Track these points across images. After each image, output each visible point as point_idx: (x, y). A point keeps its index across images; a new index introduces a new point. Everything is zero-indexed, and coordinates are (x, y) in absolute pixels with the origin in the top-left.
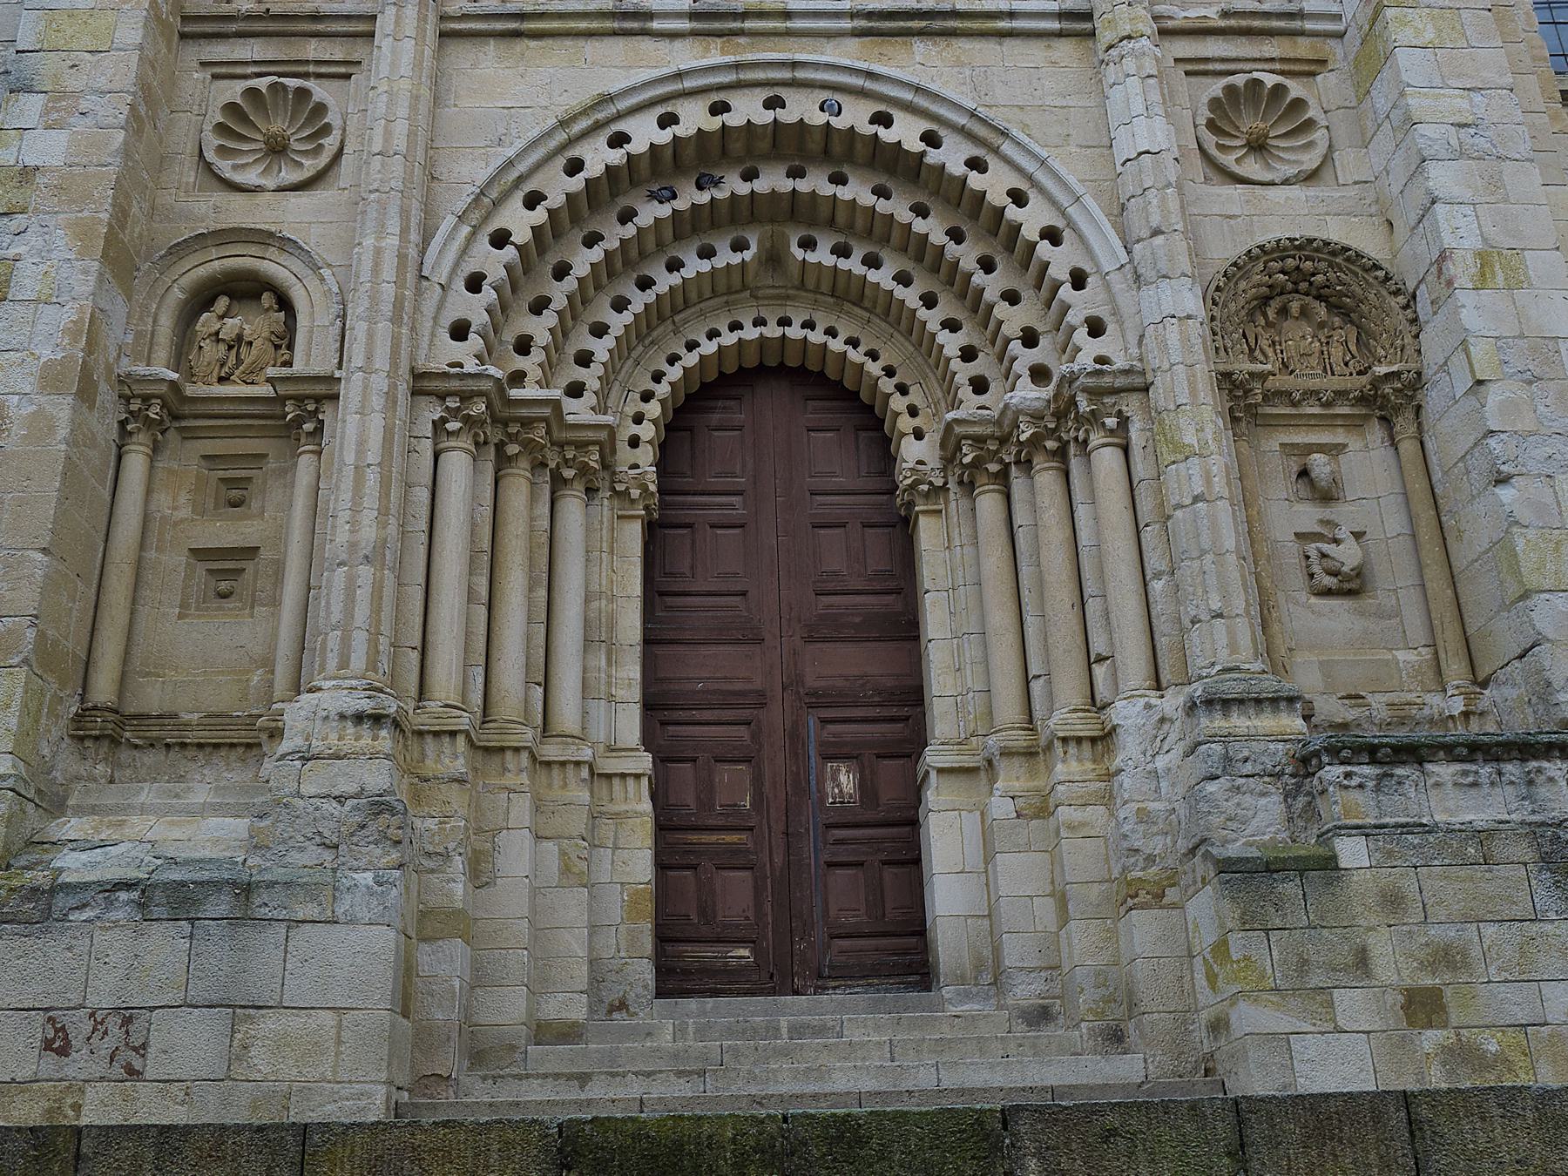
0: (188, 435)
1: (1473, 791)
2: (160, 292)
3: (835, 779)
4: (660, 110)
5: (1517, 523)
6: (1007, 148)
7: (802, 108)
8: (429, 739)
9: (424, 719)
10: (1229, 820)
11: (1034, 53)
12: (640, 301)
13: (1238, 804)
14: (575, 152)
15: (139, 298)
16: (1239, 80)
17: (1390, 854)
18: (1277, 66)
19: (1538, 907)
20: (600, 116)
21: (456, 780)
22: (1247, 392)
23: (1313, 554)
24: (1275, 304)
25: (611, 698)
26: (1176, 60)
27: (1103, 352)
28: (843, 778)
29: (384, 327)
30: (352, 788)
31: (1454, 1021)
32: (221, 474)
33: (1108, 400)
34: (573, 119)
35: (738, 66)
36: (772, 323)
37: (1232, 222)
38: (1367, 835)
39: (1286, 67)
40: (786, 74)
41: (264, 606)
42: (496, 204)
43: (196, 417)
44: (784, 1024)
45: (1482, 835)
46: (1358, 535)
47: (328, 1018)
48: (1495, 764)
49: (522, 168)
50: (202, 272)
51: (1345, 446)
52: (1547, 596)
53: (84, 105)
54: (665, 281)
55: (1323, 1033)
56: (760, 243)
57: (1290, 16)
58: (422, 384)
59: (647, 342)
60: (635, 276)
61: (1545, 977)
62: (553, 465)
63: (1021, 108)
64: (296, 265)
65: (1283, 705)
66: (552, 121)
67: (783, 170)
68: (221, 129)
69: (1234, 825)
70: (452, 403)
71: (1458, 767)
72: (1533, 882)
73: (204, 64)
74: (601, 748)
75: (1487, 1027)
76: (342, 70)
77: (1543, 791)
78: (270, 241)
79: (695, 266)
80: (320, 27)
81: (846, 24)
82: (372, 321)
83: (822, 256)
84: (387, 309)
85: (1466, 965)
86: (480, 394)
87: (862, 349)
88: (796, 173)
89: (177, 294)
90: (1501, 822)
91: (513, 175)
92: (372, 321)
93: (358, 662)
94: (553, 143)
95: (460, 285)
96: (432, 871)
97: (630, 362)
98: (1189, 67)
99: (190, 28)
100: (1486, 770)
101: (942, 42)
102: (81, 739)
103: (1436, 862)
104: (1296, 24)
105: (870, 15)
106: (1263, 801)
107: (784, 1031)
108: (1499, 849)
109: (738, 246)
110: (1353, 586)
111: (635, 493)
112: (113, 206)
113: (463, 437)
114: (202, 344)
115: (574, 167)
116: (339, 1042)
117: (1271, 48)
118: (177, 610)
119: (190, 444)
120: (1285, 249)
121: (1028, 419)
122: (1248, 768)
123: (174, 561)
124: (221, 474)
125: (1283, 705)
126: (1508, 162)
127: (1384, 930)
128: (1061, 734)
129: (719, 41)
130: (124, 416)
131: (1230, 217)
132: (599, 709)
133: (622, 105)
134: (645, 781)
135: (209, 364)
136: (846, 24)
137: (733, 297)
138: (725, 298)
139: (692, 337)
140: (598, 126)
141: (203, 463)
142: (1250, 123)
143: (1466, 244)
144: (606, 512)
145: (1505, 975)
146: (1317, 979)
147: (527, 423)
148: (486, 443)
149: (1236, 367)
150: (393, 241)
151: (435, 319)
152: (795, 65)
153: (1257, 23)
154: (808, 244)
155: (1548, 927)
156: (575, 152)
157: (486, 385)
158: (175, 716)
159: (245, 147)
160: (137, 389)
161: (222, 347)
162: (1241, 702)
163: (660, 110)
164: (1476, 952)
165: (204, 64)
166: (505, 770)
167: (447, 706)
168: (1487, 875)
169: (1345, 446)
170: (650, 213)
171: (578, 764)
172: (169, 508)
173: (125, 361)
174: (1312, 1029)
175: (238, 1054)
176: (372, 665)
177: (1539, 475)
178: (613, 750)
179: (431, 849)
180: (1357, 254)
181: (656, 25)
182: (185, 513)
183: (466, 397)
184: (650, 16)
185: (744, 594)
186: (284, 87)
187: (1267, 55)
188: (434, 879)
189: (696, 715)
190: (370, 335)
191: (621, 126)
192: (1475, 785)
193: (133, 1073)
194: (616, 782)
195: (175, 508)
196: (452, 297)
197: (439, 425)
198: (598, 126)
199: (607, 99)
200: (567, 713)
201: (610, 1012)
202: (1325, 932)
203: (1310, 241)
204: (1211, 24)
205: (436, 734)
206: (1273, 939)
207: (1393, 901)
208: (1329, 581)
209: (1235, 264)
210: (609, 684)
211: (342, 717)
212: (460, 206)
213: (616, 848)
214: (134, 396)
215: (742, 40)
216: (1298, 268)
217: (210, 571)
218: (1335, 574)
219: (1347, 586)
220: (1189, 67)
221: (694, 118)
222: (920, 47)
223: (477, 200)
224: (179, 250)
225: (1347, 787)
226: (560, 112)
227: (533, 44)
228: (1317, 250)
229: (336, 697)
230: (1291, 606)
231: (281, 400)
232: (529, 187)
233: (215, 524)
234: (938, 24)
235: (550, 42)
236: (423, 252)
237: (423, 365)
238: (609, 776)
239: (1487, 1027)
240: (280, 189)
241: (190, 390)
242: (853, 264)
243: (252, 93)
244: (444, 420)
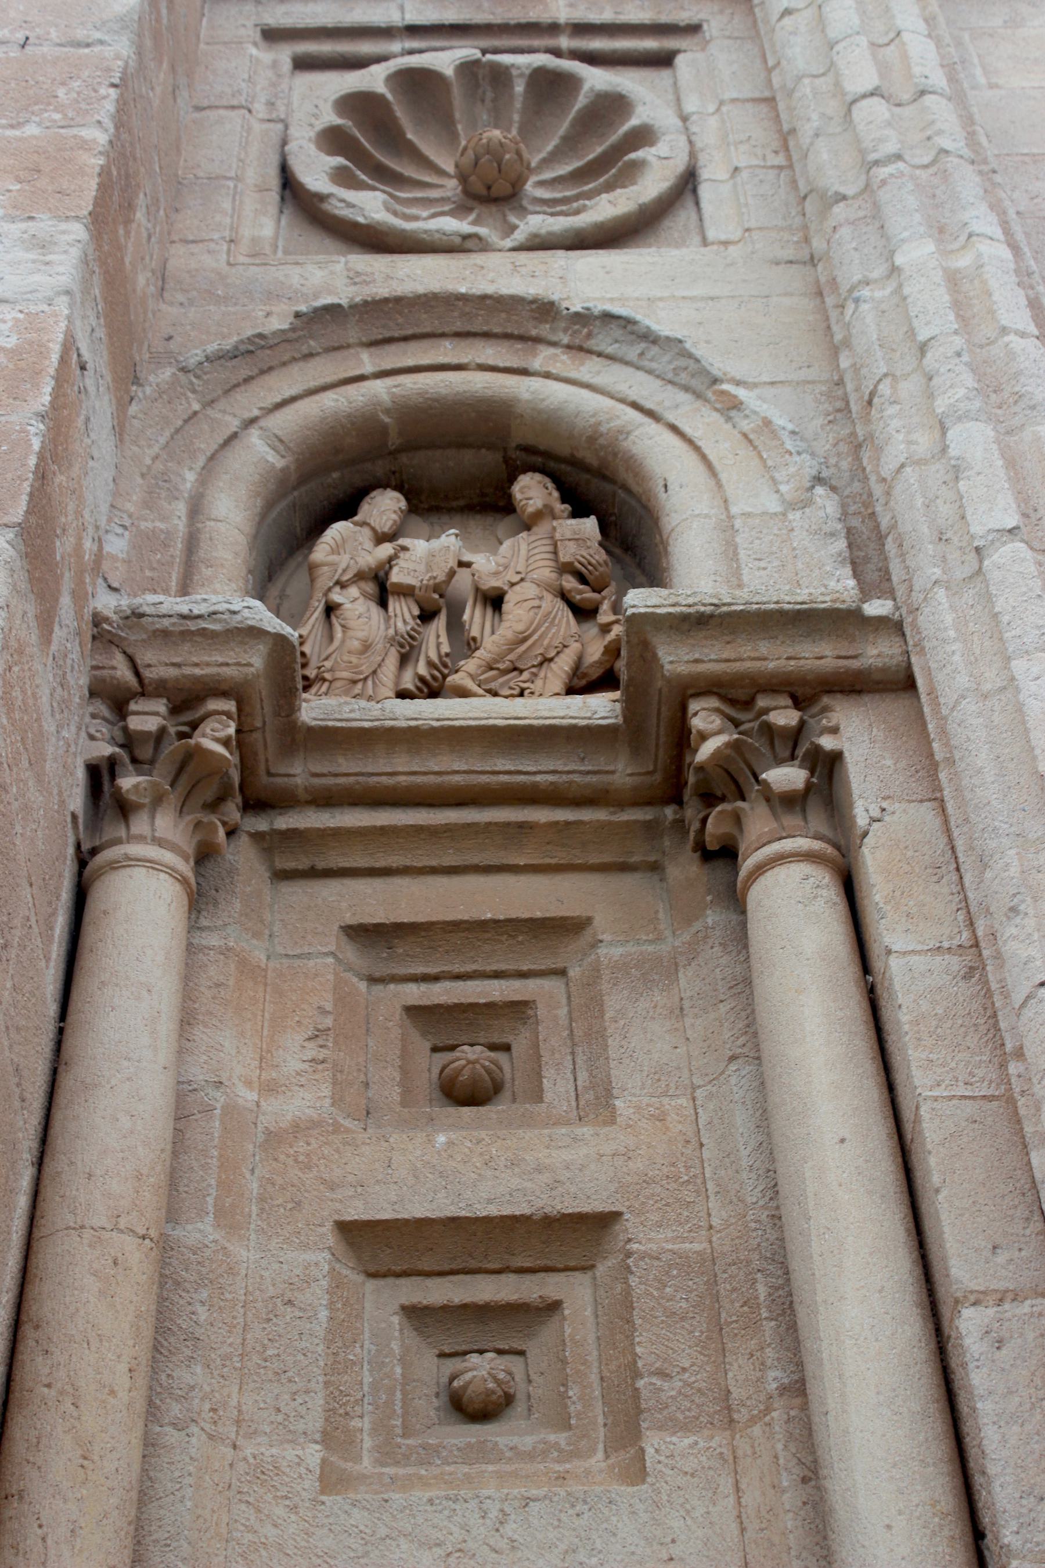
2: (207, 444)
32: (415, 994)
41: (685, 1427)
50: (333, 402)
73: (272, 35)
76: (649, 44)
78: (543, 330)
114: (336, 597)
119: (297, 893)
124: (415, 994)
130: (108, 750)
135: (366, 647)
141: (350, 953)
161: (404, 613)
165: (272, 35)
172: (248, 1084)
186: (500, 76)
195: (270, 1088)
214: (145, 690)
233: (430, 1141)
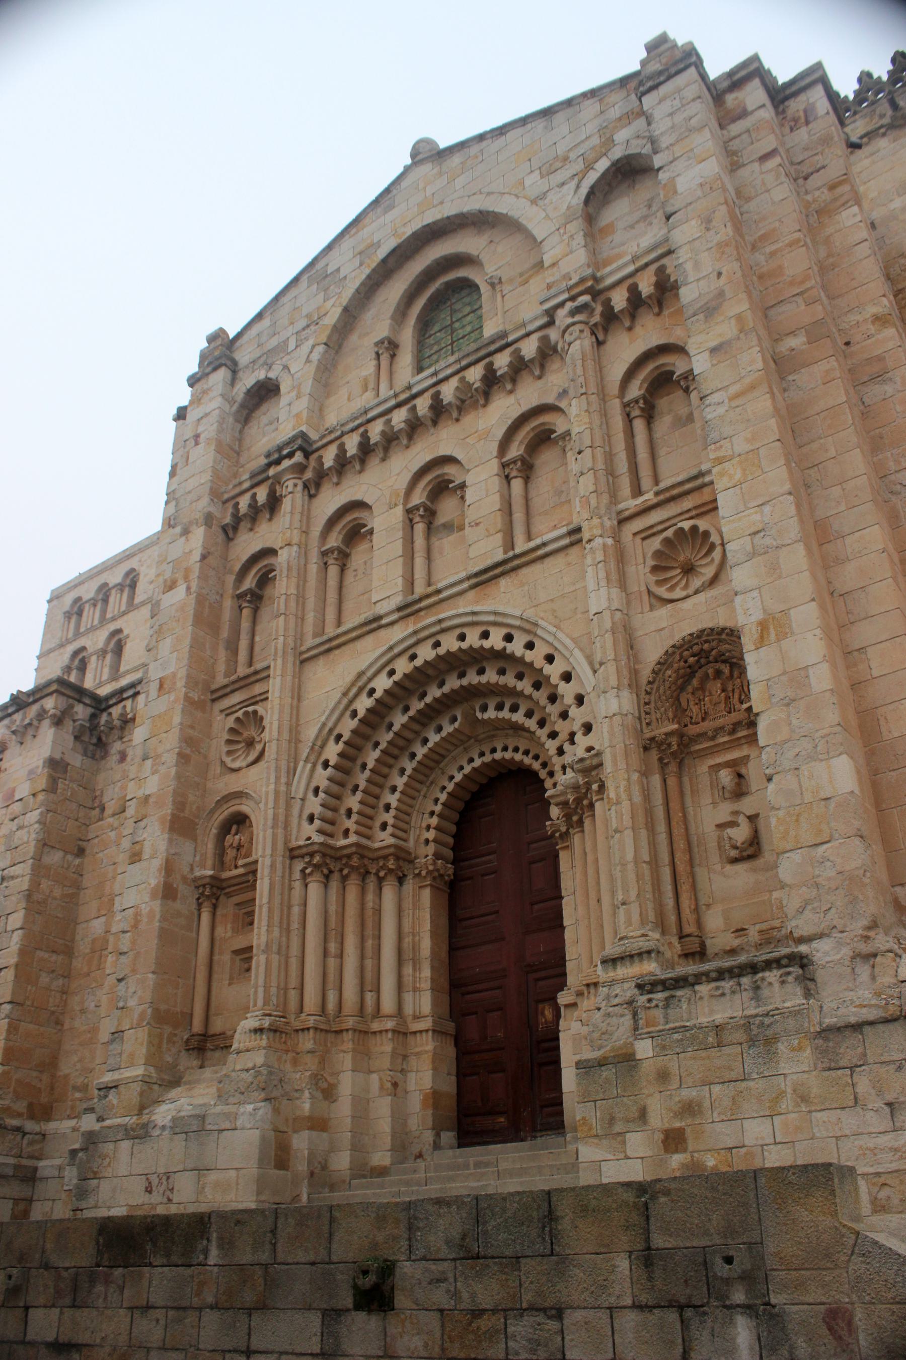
0: (229, 895)
1: (722, 999)
3: (543, 1014)
4: (388, 669)
5: (773, 808)
6: (539, 632)
7: (450, 644)
8: (300, 1032)
9: (297, 1023)
10: (603, 1034)
11: (558, 561)
12: (409, 766)
13: (608, 1024)
14: (352, 708)
15: (199, 839)
16: (669, 533)
17: (664, 1047)
18: (694, 513)
19: (746, 1071)
20: (360, 684)
21: (309, 1052)
22: (669, 745)
23: (726, 837)
24: (699, 674)
25: (415, 990)
26: (635, 534)
27: (589, 744)
28: (546, 1012)
29: (269, 832)
30: (250, 1065)
31: (690, 1148)
33: (594, 773)
34: (349, 690)
35: (415, 632)
36: (487, 753)
37: (662, 632)
38: (653, 1037)
39: (698, 511)
40: (437, 628)
42: (322, 747)
43: (229, 887)
44: (471, 1161)
45: (718, 1028)
46: (753, 819)
47: (233, 1173)
48: (736, 980)
49: (330, 724)
50: (221, 817)
51: (748, 756)
52: (787, 855)
53: (163, 759)
54: (421, 751)
55: (618, 1160)
56: (463, 714)
57: (695, 478)
58: (293, 854)
59: (428, 784)
60: (407, 754)
61: (746, 1116)
62: (374, 871)
63: (552, 600)
64: (251, 803)
65: (645, 956)
66: (339, 695)
67: (455, 675)
68: (229, 742)
69: (605, 1037)
70: (307, 859)
71: (713, 985)
72: (745, 1055)
73: (222, 711)
74: (410, 1018)
75: (709, 1150)
77: (765, 992)
79: (434, 739)
80: (258, 677)
81: (465, 585)
82: (265, 831)
83: (491, 714)
84: (270, 823)
85: (700, 1112)
86: (316, 852)
87: (531, 755)
88: (441, 684)
89: (214, 831)
90: (731, 1018)
91: (327, 729)
92: (265, 831)
93: (260, 1002)
94: (342, 707)
95: (310, 795)
96: (297, 1099)
97: (421, 798)
98: (643, 535)
99: (214, 696)
100: (727, 985)
101: (513, 574)
102: (188, 1050)
103: (690, 1049)
104: (699, 482)
105: (476, 575)
106: (622, 1019)
107: (472, 1166)
108: (727, 1037)
109: (454, 719)
110: (750, 851)
111: (424, 873)
112: (173, 805)
113: (315, 874)
115: (354, 714)
116: (237, 1184)
117: (687, 503)
118: (227, 982)
120: (690, 641)
121: (571, 790)
122: (616, 1001)
123: (227, 957)
124: (244, 911)
125: (645, 956)
126: (784, 548)
127: (657, 1095)
128: (584, 983)
129: (412, 618)
131: (661, 630)
132: (408, 997)
133: (369, 674)
134: (430, 1033)
136: (465, 585)
137: (466, 745)
138: (462, 747)
139: (451, 773)
140: (361, 689)
142: (685, 554)
143: (754, 619)
144: (411, 885)
145: (723, 1117)
146: (618, 1128)
147: (349, 857)
148: (331, 872)
149: (656, 732)
150: (272, 787)
151: (300, 816)
152: (440, 621)
153: (675, 492)
154: (484, 709)
155: (751, 1084)
156: (352, 708)
157: (316, 848)
158: (224, 1033)
159: (240, 746)
160: (200, 882)
161: (235, 851)
162: (622, 958)
163: (388, 669)
164: (707, 1104)
166: (344, 1041)
167: (308, 1015)
168: (719, 1054)
169: (748, 756)
170: (399, 720)
171: (387, 1031)
173: (196, 869)
174: (612, 1157)
175: (201, 1191)
176: (266, 1002)
177: (790, 770)
178: (418, 1018)
179: (296, 1088)
180: (732, 630)
181: (384, 622)
182: (229, 934)
183: (312, 855)
184: (380, 618)
185: (497, 912)
187: (685, 509)
188: (298, 1102)
189: (470, 988)
190: (265, 838)
191: (369, 686)
192: (723, 995)
193: (170, 1200)
194: (418, 1035)
195: (226, 932)
196: (307, 803)
197: (303, 871)
198: (361, 689)
199: (361, 674)
200: (388, 1004)
201: (415, 1159)
202: (625, 1099)
203: (703, 631)
204: (650, 503)
205: (303, 1030)
206: (598, 1106)
207: (663, 1076)
208: (734, 853)
209: (659, 663)
210: (414, 982)
211: (250, 1031)
212: (305, 755)
213: (417, 1071)
215: (422, 613)
216: (702, 649)
217: (242, 960)
218: (736, 848)
219: (745, 854)
220: (643, 535)
221: (403, 667)
222: (503, 582)
223: (312, 748)
224: (212, 812)
225: (649, 1008)
226: (343, 689)
227: (337, 652)
228: (708, 635)
229: (251, 1022)
230: (711, 875)
231: (248, 873)
232: (335, 733)
234: (508, 567)
235: (344, 648)
236: (289, 784)
237: (294, 844)
238: (415, 1033)
239: (709, 1150)
240: (248, 766)
241: (226, 875)
242: (505, 714)
243: (238, 720)
244: (306, 868)
